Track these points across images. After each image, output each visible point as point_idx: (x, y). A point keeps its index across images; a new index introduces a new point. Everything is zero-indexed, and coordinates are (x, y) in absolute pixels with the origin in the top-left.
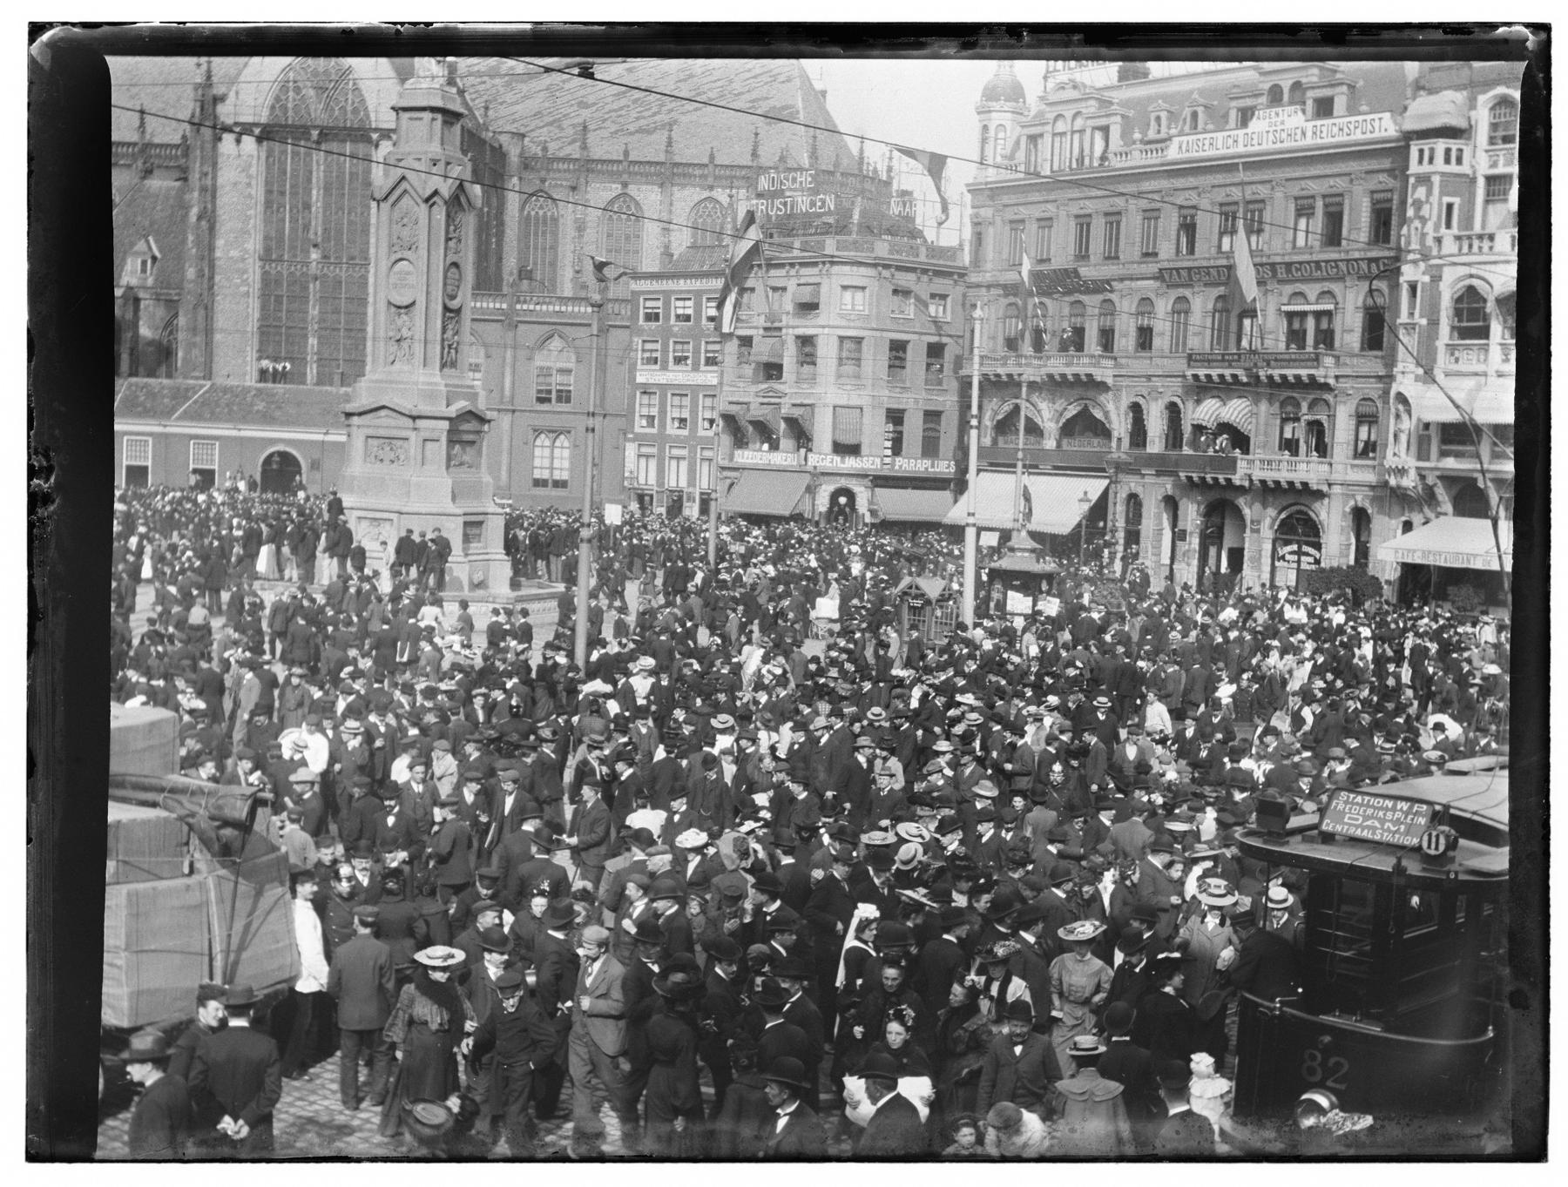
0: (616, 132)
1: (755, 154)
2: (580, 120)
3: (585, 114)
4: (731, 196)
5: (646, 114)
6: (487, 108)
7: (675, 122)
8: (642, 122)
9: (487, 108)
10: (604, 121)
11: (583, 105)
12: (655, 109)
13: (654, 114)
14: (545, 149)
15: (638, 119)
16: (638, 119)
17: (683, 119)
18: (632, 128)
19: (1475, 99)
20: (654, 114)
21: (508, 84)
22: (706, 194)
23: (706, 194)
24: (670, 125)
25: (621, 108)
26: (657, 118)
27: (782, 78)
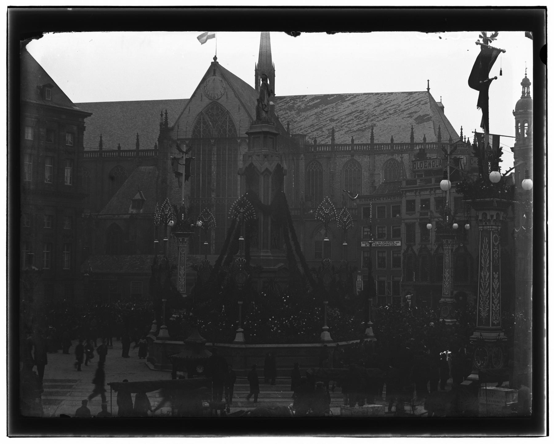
0: (348, 131)
1: (412, 138)
5: (362, 122)
6: (288, 125)
7: (375, 125)
8: (359, 126)
9: (288, 125)
10: (342, 127)
11: (332, 120)
13: (365, 122)
14: (315, 141)
15: (357, 125)
17: (378, 124)
18: (355, 129)
19: (411, 141)
20: (365, 122)
22: (390, 157)
23: (390, 157)
26: (367, 124)
27: (422, 103)
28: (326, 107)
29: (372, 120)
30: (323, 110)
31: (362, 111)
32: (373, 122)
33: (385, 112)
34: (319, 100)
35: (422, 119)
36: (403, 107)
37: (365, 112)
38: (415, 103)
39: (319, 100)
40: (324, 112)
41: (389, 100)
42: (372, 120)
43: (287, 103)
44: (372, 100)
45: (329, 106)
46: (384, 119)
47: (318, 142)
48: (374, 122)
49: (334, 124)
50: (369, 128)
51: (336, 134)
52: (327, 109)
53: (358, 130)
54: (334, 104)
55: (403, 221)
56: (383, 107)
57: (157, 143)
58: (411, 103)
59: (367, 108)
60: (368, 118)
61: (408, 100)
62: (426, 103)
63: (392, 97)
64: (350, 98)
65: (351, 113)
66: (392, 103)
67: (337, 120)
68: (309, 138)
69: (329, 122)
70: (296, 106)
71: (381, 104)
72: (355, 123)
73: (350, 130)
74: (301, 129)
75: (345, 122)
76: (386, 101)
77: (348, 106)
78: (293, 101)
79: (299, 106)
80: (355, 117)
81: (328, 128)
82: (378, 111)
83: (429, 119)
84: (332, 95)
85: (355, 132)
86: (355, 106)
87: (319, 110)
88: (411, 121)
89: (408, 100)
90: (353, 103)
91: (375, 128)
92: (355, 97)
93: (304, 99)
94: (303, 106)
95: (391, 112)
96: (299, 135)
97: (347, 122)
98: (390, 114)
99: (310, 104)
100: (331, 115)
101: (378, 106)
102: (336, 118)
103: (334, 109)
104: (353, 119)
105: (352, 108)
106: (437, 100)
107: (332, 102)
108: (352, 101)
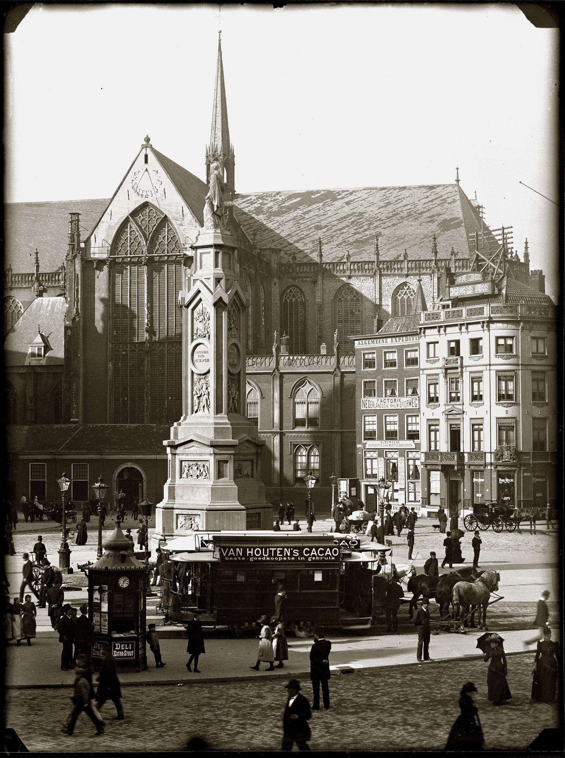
0: (341, 244)
2: (316, 237)
3: (320, 234)
4: (420, 281)
5: (362, 230)
7: (380, 233)
8: (358, 236)
9: (255, 235)
10: (332, 237)
11: (318, 228)
12: (366, 227)
13: (366, 230)
14: (294, 258)
15: (355, 234)
16: (355, 234)
20: (366, 230)
21: (269, 217)
24: (377, 236)
25: (344, 228)
27: (449, 200)
28: (310, 208)
29: (376, 227)
30: (304, 214)
31: (361, 214)
32: (377, 230)
33: (394, 215)
34: (298, 199)
35: (447, 225)
36: (420, 208)
37: (366, 215)
38: (438, 202)
39: (298, 199)
40: (307, 216)
41: (400, 197)
42: (376, 227)
43: (252, 203)
44: (377, 198)
45: (314, 206)
46: (394, 225)
47: (298, 259)
48: (379, 230)
49: (320, 234)
50: (372, 237)
51: (325, 248)
52: (310, 211)
53: (357, 241)
54: (321, 204)
55: (421, 372)
56: (390, 208)
57: (65, 262)
58: (432, 201)
59: (369, 209)
60: (370, 224)
61: (428, 197)
62: (454, 201)
63: (405, 193)
64: (343, 195)
65: (345, 217)
66: (404, 203)
67: (326, 226)
68: (285, 254)
69: (313, 230)
70: (265, 207)
71: (389, 203)
72: (352, 231)
73: (345, 242)
74: (274, 241)
75: (336, 230)
76: (396, 199)
77: (342, 207)
78: (261, 201)
79: (271, 207)
80: (352, 222)
81: (312, 239)
82: (386, 212)
83: (458, 225)
84: (318, 192)
85: (351, 244)
86: (351, 206)
87: (299, 212)
88: (433, 227)
89: (428, 197)
90: (348, 203)
91: (380, 238)
92: (351, 194)
93: (278, 197)
94: (275, 208)
95: (402, 214)
96: (270, 249)
97: (340, 230)
98: (402, 218)
99: (286, 204)
100: (317, 219)
101: (385, 206)
102: (323, 224)
103: (322, 212)
104: (348, 226)
105: (347, 210)
106: (470, 196)
107: (316, 201)
108: (346, 200)
